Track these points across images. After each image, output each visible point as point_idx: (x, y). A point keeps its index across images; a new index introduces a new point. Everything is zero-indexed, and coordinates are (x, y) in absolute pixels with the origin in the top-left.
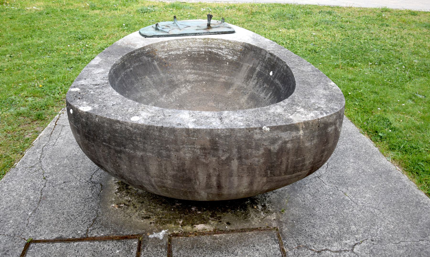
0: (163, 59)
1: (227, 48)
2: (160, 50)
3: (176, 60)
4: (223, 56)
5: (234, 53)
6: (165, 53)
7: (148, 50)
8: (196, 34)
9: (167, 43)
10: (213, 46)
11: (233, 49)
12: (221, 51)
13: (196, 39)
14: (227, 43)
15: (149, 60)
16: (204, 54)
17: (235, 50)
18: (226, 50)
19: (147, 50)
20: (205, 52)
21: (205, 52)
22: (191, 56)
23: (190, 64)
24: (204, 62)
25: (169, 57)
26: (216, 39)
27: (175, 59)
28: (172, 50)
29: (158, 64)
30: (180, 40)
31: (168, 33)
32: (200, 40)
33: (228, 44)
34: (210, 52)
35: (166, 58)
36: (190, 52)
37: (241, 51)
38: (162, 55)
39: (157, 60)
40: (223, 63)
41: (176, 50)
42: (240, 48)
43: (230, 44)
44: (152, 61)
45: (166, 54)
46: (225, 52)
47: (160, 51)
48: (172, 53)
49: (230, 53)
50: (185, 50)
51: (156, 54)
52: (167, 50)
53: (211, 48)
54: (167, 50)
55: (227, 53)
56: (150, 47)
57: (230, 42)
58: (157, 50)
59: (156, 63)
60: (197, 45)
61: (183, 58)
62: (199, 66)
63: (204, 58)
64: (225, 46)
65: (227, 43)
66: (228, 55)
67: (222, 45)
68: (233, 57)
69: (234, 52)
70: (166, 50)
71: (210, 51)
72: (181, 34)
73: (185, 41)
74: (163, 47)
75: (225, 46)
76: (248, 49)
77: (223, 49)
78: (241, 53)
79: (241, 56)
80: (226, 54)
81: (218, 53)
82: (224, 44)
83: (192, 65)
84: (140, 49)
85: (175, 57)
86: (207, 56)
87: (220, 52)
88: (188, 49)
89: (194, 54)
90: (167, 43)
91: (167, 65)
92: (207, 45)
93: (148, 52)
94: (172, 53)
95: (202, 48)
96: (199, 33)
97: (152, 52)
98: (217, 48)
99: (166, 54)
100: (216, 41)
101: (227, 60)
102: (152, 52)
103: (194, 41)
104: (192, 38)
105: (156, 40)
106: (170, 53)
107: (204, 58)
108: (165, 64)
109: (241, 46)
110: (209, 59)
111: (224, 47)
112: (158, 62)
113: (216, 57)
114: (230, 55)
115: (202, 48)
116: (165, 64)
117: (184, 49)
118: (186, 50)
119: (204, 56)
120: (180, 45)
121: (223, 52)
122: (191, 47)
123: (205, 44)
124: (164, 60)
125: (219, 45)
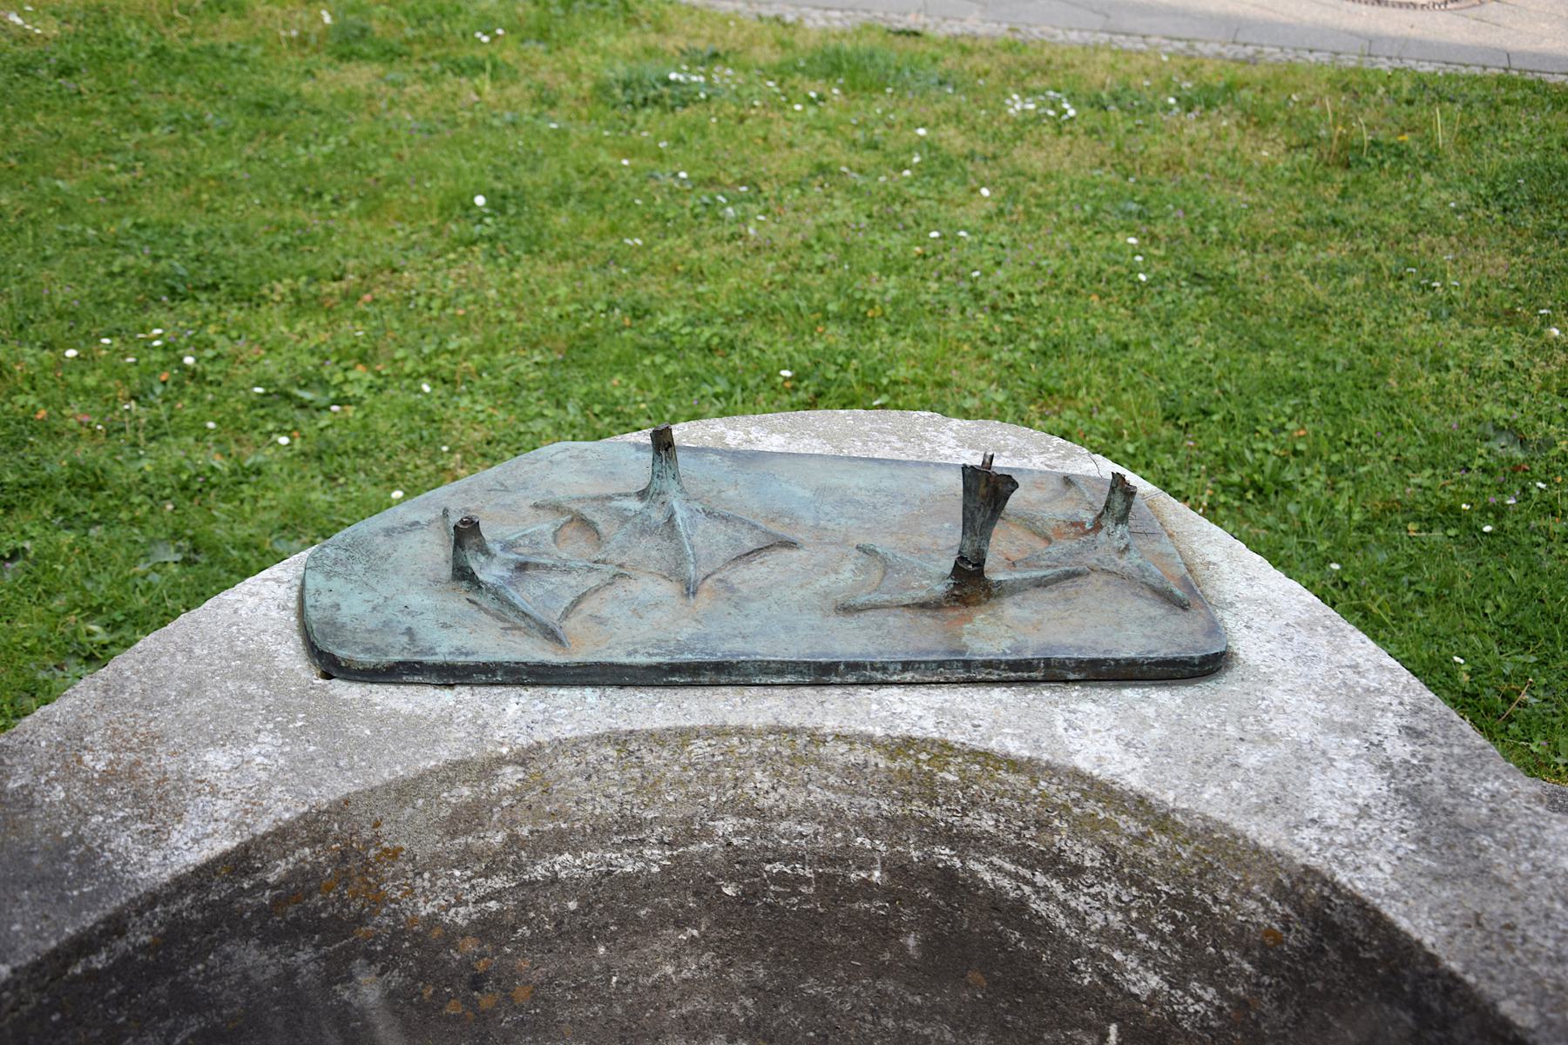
0: (452, 935)
1: (1116, 866)
2: (434, 843)
3: (589, 934)
4: (1076, 949)
5: (1189, 944)
6: (488, 873)
7: (296, 874)
8: (821, 674)
9: (511, 776)
10: (987, 823)
11: (1187, 903)
12: (1057, 887)
13: (816, 738)
14: (1133, 826)
15: (290, 974)
16: (886, 892)
17: (1206, 919)
18: (1111, 889)
19: (279, 870)
20: (898, 869)
21: (898, 869)
22: (749, 897)
23: (736, 977)
24: (880, 971)
25: (523, 906)
26: (1015, 765)
27: (586, 930)
28: (561, 841)
29: (391, 996)
30: (656, 738)
31: (551, 635)
32: (858, 756)
33: (1141, 839)
34: (948, 880)
35: (486, 928)
36: (738, 861)
37: (1266, 952)
38: (447, 899)
39: (383, 957)
40: (1064, 1023)
41: (600, 833)
42: (1258, 911)
43: (1160, 840)
44: (337, 972)
45: (497, 882)
46: (1095, 907)
47: (436, 861)
48: (565, 863)
49: (1153, 933)
50: (692, 837)
51: (381, 900)
52: (513, 839)
53: (963, 840)
54: (513, 839)
55: (1116, 920)
56: (317, 840)
57: (1163, 821)
58: (395, 854)
59: (368, 989)
60: (818, 796)
61: (664, 918)
62: (819, 1004)
63: (885, 932)
64: (1110, 852)
65: (1133, 826)
66: (1129, 946)
67: (1075, 834)
68: (1178, 980)
69: (1197, 938)
70: (498, 838)
71: (949, 872)
72: (675, 669)
73: (699, 748)
74: (469, 817)
75: (1110, 852)
76: (1349, 952)
77: (1077, 870)
78: (1263, 966)
79: (1267, 1004)
80: (1106, 933)
81: (1021, 904)
82: (1097, 824)
83: (754, 989)
84: (203, 875)
85: (587, 906)
86: (907, 914)
87: (1048, 899)
88: (726, 825)
89: (780, 878)
90: (511, 776)
91: (486, 1001)
92: (917, 805)
93: (301, 884)
94: (565, 863)
95: (868, 826)
96: (853, 667)
97: (345, 879)
98: (1019, 854)
99: (497, 882)
100: (1019, 781)
101: (1124, 1008)
102: (345, 879)
103: (793, 760)
104: (778, 730)
105: (413, 724)
106: (539, 872)
107: (885, 932)
108: (477, 982)
109: (1280, 892)
110: (924, 945)
111: (1091, 857)
112: (396, 978)
113: (1003, 942)
114: (1145, 956)
115: (868, 826)
116: (477, 982)
117: (689, 832)
118: (708, 834)
119: (878, 906)
120: (648, 786)
121: (1080, 903)
122: (760, 813)
123: (906, 798)
124: (470, 945)
125: (1042, 825)
